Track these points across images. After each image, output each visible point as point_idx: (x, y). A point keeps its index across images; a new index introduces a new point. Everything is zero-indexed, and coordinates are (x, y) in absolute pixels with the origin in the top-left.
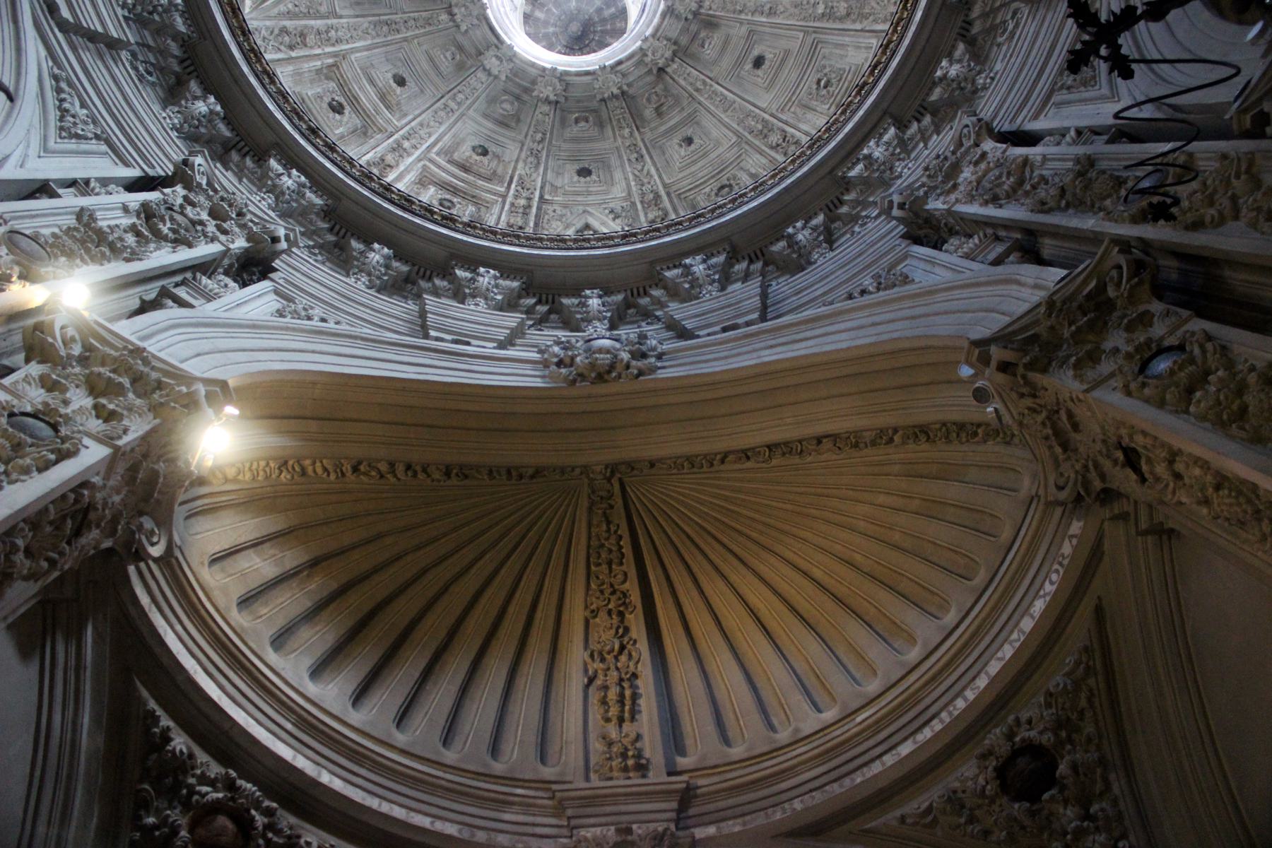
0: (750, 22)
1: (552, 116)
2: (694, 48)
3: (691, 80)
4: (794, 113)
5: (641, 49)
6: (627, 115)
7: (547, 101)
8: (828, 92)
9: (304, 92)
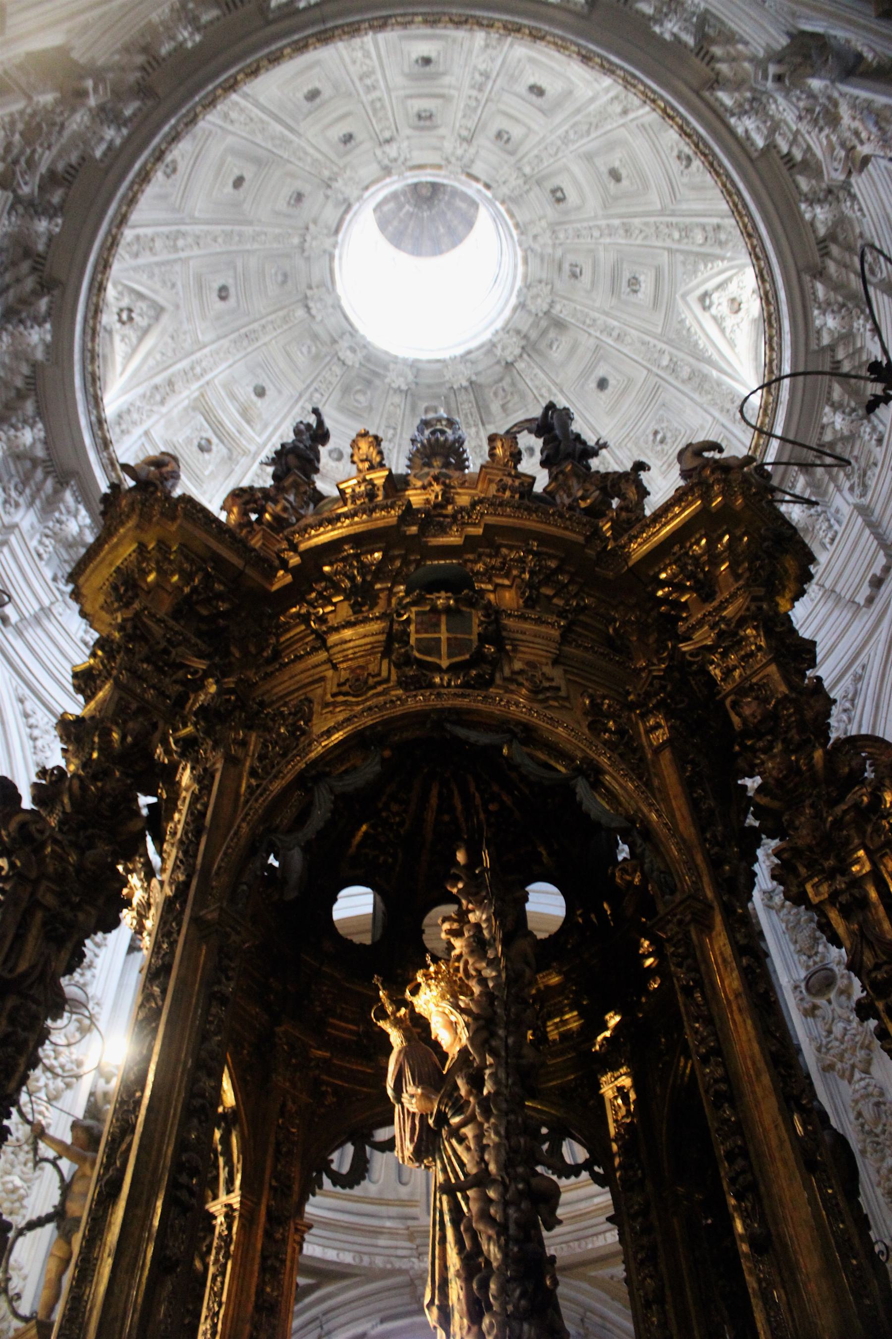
0: (597, 338)
1: (402, 406)
2: (543, 346)
3: (537, 383)
4: (630, 450)
5: (491, 341)
6: (475, 410)
7: (399, 390)
8: (663, 450)
9: (175, 439)
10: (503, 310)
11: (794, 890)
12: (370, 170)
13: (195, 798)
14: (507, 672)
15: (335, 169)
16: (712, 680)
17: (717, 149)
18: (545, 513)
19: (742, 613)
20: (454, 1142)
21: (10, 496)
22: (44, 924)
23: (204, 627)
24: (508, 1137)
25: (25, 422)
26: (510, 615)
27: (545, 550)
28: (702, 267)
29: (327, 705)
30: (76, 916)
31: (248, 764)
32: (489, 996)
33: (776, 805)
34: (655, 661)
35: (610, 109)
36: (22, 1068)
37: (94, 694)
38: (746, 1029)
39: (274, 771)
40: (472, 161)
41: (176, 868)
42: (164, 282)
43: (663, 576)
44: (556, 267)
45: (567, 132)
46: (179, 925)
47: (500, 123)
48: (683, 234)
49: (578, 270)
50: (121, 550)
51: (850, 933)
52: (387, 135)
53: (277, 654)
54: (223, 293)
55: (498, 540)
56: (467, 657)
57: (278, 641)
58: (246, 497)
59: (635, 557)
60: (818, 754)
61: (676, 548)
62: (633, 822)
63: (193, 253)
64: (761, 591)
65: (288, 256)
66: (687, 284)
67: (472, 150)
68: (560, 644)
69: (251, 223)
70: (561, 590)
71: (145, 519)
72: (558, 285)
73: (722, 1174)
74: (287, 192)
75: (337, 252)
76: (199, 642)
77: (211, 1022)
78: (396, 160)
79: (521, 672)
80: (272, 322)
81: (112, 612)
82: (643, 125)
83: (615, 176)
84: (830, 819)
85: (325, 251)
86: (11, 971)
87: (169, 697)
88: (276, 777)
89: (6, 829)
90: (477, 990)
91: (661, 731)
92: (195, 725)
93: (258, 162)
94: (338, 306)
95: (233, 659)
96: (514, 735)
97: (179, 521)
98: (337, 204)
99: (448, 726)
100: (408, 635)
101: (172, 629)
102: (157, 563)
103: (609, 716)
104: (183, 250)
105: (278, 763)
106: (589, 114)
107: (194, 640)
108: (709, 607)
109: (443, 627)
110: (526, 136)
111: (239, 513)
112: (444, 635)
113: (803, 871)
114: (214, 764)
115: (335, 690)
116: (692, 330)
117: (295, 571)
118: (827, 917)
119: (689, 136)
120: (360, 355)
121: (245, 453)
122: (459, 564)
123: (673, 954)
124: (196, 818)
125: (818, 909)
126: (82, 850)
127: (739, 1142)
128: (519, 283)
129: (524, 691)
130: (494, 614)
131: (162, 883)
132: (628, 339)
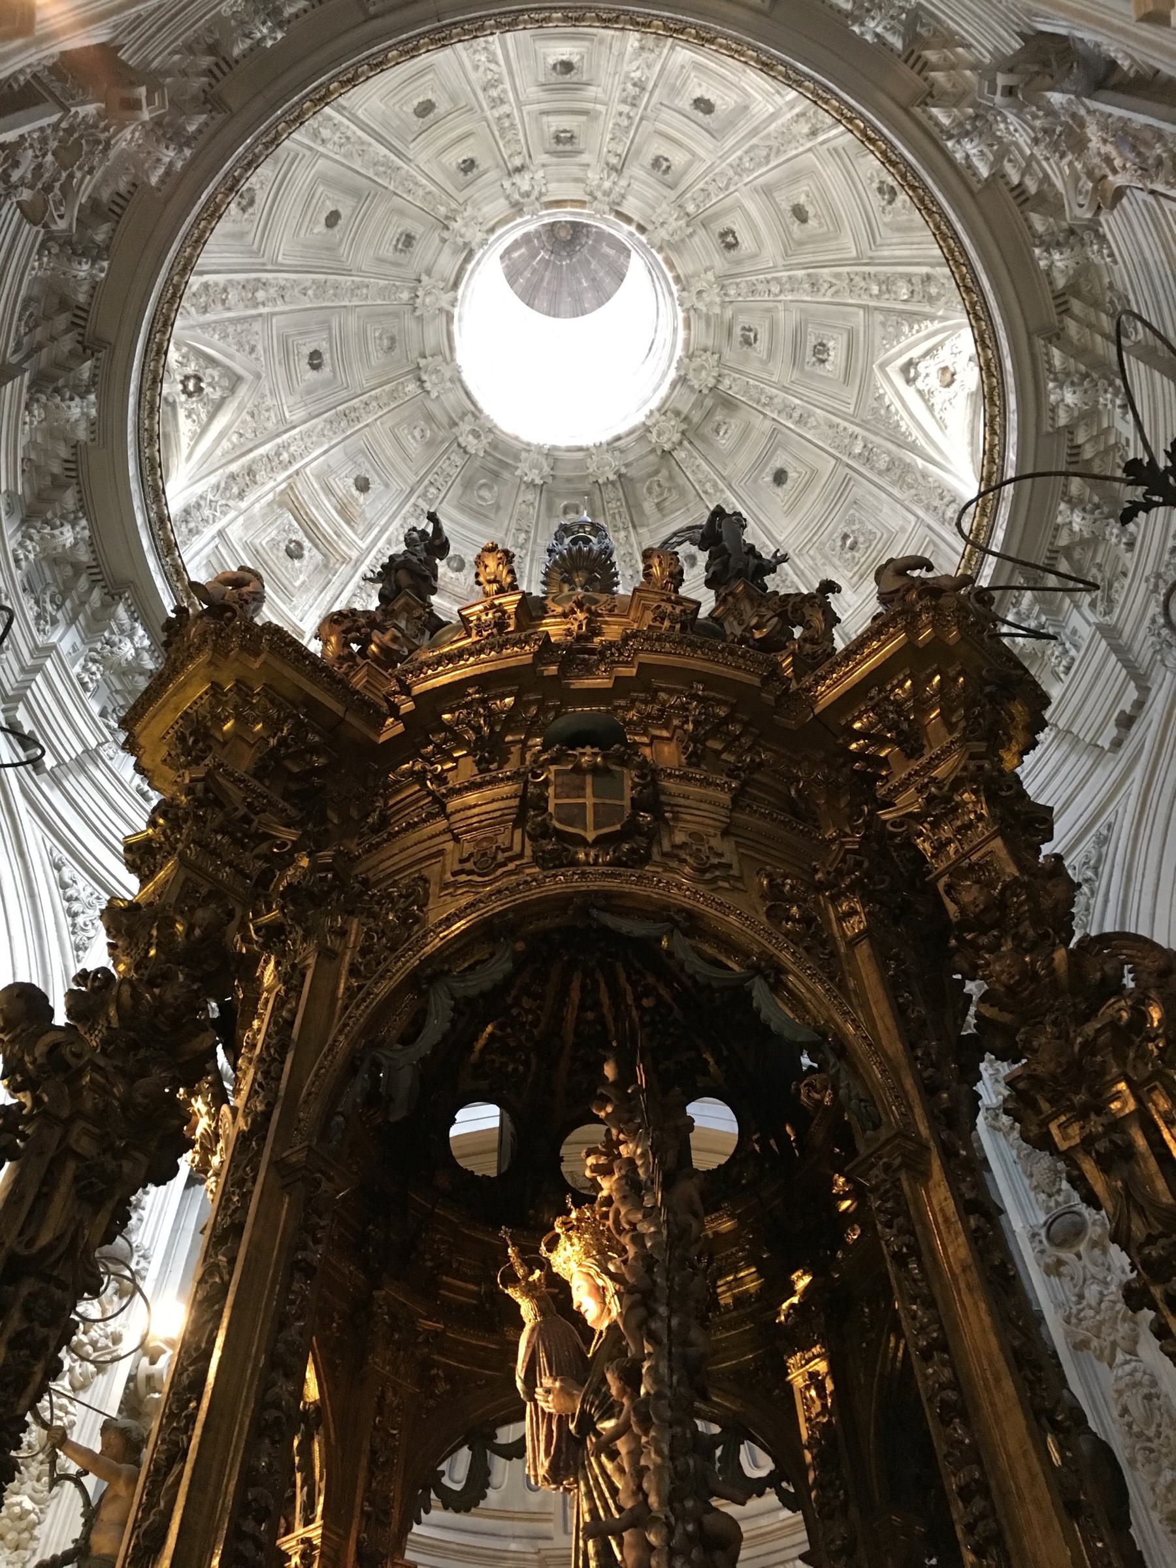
2: (707, 430)
3: (700, 476)
4: (812, 558)
6: (624, 509)
9: (257, 542)
10: (659, 386)
11: (1034, 1130)
12: (497, 208)
13: (281, 1002)
14: (666, 846)
15: (454, 206)
16: (920, 856)
17: (929, 181)
18: (713, 649)
19: (957, 773)
20: (603, 1458)
21: (45, 610)
22: (76, 1179)
23: (293, 787)
24: (672, 1459)
25: (64, 517)
26: (670, 776)
27: (712, 694)
28: (906, 329)
29: (446, 886)
30: (121, 1166)
31: (347, 959)
32: (647, 1260)
33: (1006, 1017)
34: (848, 830)
35: (795, 129)
36: (38, 1378)
37: (153, 873)
38: (979, 1315)
39: (381, 968)
40: (623, 196)
41: (253, 1093)
42: (241, 345)
43: (857, 725)
44: (725, 333)
45: (740, 159)
46: (256, 1170)
47: (658, 148)
48: (884, 287)
49: (752, 335)
50: (189, 691)
51: (1112, 1191)
52: (517, 162)
53: (384, 821)
54: (315, 360)
55: (656, 683)
56: (618, 827)
57: (386, 804)
58: (347, 624)
59: (823, 704)
60: (1060, 955)
61: (874, 692)
62: (824, 1036)
63: (277, 309)
64: (981, 747)
65: (396, 315)
66: (887, 351)
67: (623, 183)
68: (731, 811)
69: (348, 272)
70: (731, 742)
71: (221, 651)
72: (727, 353)
73: (955, 1517)
74: (393, 232)
75: (456, 312)
76: (288, 806)
77: (293, 1302)
78: (527, 195)
79: (684, 846)
80: (376, 398)
81: (177, 768)
82: (835, 150)
83: (800, 214)
84: (1079, 1040)
85: (440, 310)
86: (29, 1244)
87: (248, 877)
88: (382, 977)
89: (31, 1053)
90: (631, 1251)
91: (857, 918)
92: (282, 908)
93: (356, 193)
94: (457, 380)
95: (330, 826)
96: (676, 924)
97: (263, 656)
98: (456, 251)
99: (594, 912)
100: (546, 800)
101: (253, 791)
102: (235, 707)
103: (792, 901)
104: (264, 304)
105: (385, 959)
106: (768, 136)
107: (282, 804)
108: (915, 765)
109: (589, 790)
110: (690, 164)
111: (338, 641)
112: (589, 801)
113: (1045, 1107)
114: (305, 958)
115: (457, 867)
116: (893, 409)
117: (407, 719)
118: (1079, 1168)
119: (894, 164)
120: (484, 441)
121: (345, 560)
122: (608, 711)
123: (878, 1209)
124: (281, 1028)
125: (1067, 1156)
126: (131, 1078)
127: (977, 1475)
128: (679, 352)
129: (687, 870)
130: (650, 774)
131: (234, 1110)
132: (812, 421)
